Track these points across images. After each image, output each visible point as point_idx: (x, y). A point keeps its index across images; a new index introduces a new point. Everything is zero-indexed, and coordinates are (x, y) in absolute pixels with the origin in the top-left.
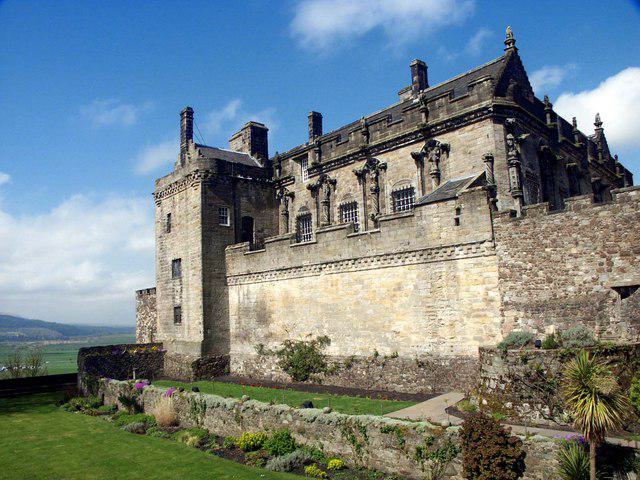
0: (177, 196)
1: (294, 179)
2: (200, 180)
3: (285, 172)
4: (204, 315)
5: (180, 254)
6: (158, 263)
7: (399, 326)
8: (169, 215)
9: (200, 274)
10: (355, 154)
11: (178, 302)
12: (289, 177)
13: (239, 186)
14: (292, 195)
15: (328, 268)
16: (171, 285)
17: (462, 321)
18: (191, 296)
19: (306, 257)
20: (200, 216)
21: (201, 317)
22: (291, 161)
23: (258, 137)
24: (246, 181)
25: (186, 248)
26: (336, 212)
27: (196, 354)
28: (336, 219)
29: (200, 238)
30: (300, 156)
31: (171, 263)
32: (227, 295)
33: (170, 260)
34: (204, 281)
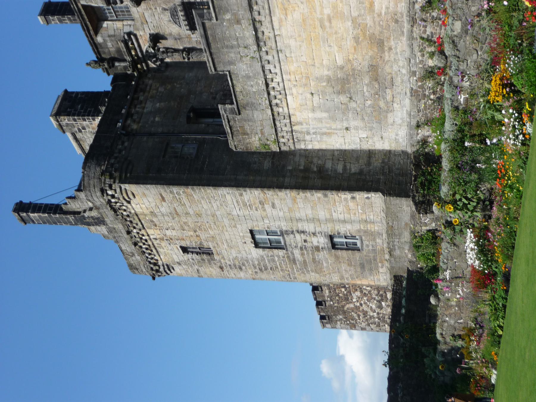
0: (153, 233)
1: (129, 34)
2: (116, 186)
3: (119, 51)
4: (339, 188)
5: (243, 230)
6: (264, 276)
11: (323, 241)
12: (125, 42)
13: (135, 127)
14: (156, 39)
16: (297, 253)
18: (309, 212)
20: (175, 189)
22: (99, 39)
23: (73, 104)
24: (129, 115)
25: (234, 220)
27: (405, 207)
29: (210, 191)
31: (260, 251)
33: (256, 253)
34: (281, 186)
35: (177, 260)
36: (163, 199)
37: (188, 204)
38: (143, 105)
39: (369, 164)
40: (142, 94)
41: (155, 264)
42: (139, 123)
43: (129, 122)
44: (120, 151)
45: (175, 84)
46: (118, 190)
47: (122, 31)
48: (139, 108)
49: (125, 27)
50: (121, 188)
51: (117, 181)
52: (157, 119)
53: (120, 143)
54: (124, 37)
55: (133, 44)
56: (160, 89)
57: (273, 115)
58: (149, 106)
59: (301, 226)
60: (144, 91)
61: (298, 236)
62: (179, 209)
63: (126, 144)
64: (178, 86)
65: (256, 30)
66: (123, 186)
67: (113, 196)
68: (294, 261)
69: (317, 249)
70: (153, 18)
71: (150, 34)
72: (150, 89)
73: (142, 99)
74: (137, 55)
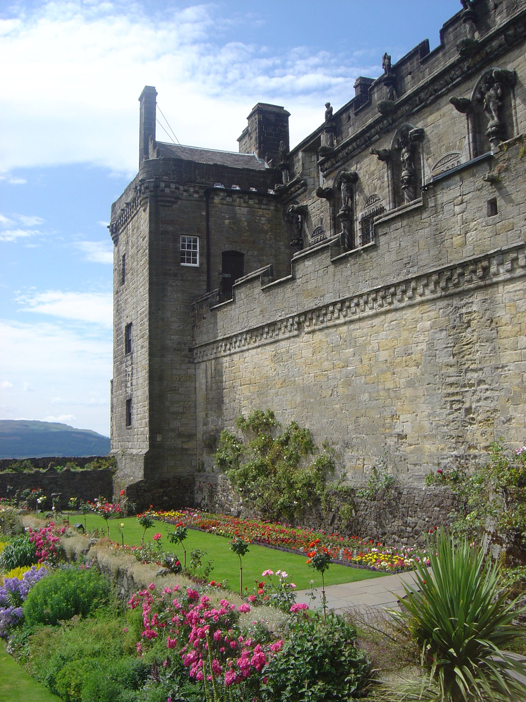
1: (305, 185)
7: (405, 424)
8: (124, 256)
9: (147, 344)
10: (377, 122)
13: (217, 200)
15: (307, 324)
17: (505, 410)
19: (288, 301)
20: (147, 251)
21: (147, 414)
22: (300, 154)
24: (230, 193)
26: (358, 226)
28: (358, 241)
30: (311, 144)
32: (193, 378)
35: (121, 248)
36: (143, 240)
37: (142, 263)
38: (243, 205)
39: (180, 435)
40: (257, 201)
41: (116, 228)
42: (222, 204)
43: (222, 194)
44: (187, 191)
45: (270, 234)
46: (145, 196)
47: (308, 177)
48: (240, 201)
49: (312, 180)
50: (147, 198)
51: (152, 194)
52: (227, 221)
53: (197, 189)
54: (302, 180)
55: (299, 189)
56: (263, 219)
57: (211, 343)
58: (242, 211)
59: (135, 371)
60: (260, 203)
61: (130, 369)
62: (139, 255)
63: (196, 196)
64: (268, 236)
65: (257, 329)
66: (148, 200)
67: (140, 190)
68: (121, 363)
69: (126, 387)
70: (317, 209)
71: (307, 205)
72: (263, 209)
73: (250, 203)
74: (292, 193)
